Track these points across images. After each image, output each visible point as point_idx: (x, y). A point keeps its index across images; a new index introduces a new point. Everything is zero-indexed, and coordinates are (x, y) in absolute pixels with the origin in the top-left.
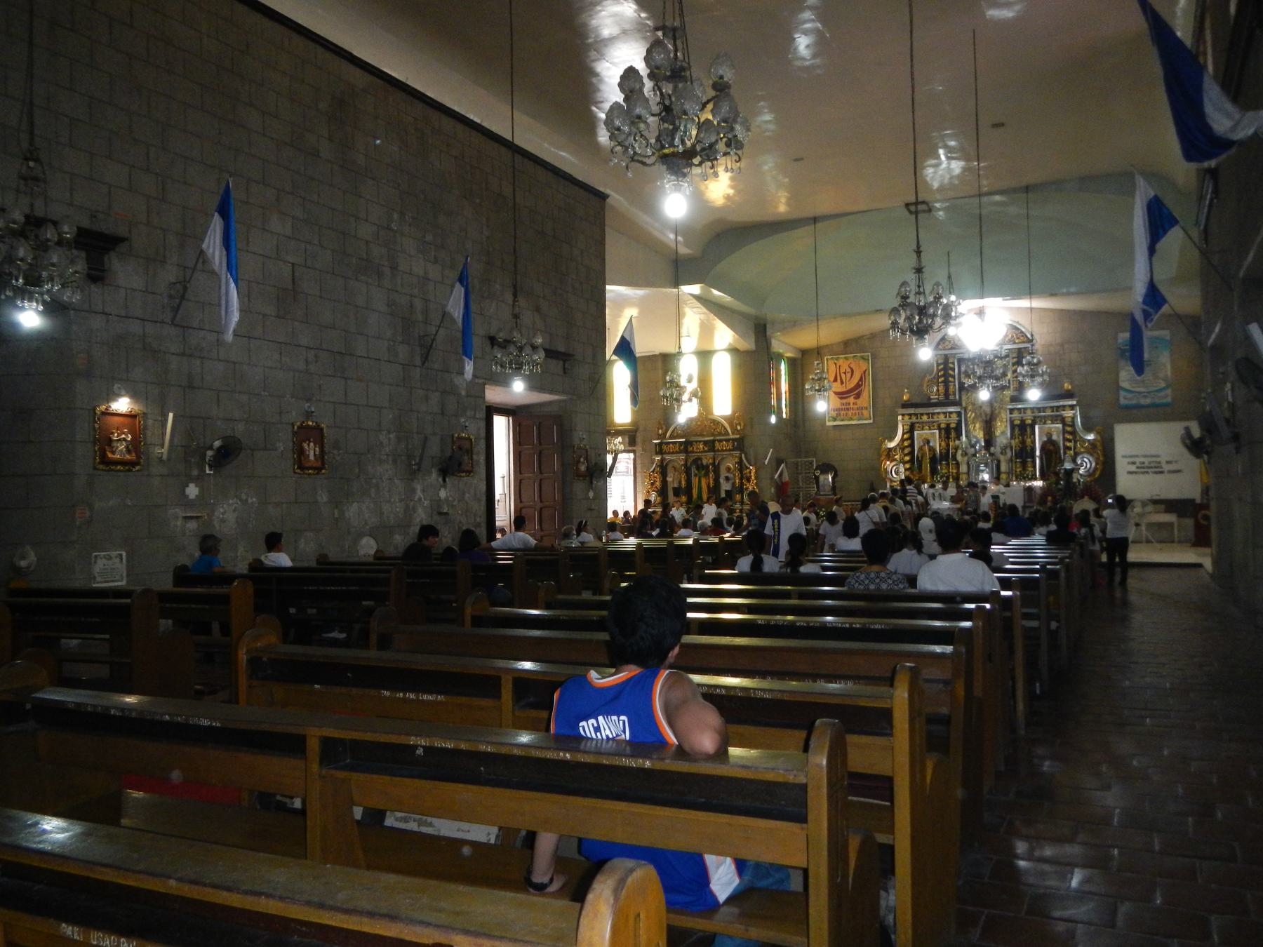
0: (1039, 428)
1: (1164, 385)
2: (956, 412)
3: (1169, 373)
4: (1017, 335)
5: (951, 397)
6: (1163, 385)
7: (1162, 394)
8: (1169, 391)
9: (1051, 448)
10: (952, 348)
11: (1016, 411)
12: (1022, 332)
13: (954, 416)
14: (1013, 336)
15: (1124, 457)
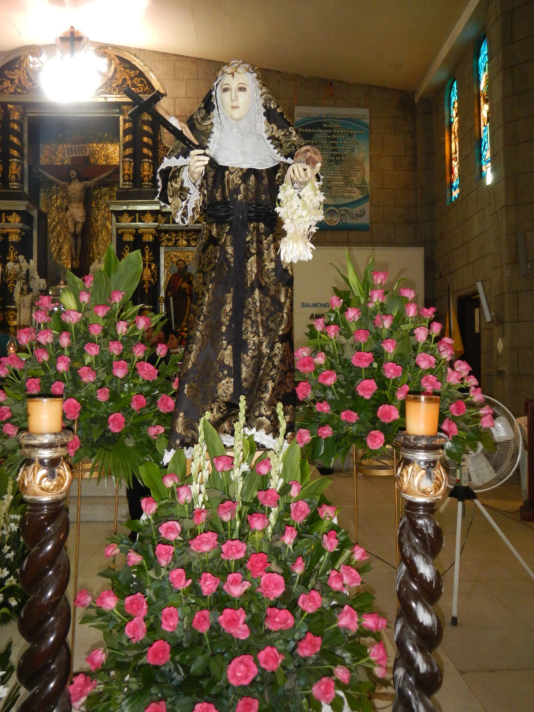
0: (165, 252)
1: (361, 197)
2: (18, 212)
3: (367, 179)
4: (132, 79)
5: (14, 185)
6: (357, 195)
7: (357, 210)
8: (366, 206)
9: (185, 285)
10: (16, 92)
11: (126, 216)
12: (141, 74)
13: (15, 219)
14: (125, 80)
15: (303, 305)
